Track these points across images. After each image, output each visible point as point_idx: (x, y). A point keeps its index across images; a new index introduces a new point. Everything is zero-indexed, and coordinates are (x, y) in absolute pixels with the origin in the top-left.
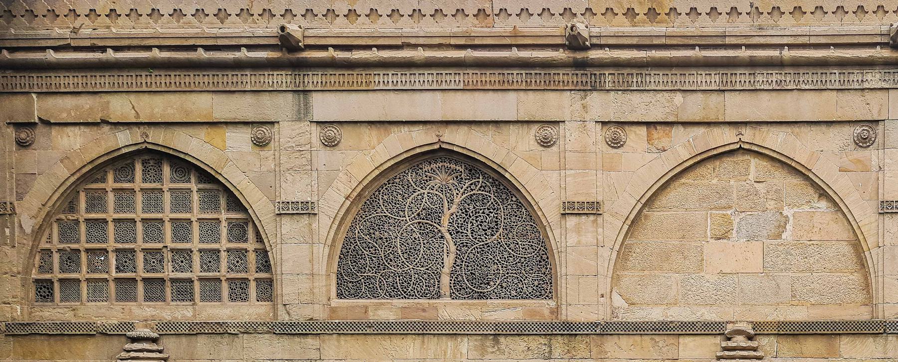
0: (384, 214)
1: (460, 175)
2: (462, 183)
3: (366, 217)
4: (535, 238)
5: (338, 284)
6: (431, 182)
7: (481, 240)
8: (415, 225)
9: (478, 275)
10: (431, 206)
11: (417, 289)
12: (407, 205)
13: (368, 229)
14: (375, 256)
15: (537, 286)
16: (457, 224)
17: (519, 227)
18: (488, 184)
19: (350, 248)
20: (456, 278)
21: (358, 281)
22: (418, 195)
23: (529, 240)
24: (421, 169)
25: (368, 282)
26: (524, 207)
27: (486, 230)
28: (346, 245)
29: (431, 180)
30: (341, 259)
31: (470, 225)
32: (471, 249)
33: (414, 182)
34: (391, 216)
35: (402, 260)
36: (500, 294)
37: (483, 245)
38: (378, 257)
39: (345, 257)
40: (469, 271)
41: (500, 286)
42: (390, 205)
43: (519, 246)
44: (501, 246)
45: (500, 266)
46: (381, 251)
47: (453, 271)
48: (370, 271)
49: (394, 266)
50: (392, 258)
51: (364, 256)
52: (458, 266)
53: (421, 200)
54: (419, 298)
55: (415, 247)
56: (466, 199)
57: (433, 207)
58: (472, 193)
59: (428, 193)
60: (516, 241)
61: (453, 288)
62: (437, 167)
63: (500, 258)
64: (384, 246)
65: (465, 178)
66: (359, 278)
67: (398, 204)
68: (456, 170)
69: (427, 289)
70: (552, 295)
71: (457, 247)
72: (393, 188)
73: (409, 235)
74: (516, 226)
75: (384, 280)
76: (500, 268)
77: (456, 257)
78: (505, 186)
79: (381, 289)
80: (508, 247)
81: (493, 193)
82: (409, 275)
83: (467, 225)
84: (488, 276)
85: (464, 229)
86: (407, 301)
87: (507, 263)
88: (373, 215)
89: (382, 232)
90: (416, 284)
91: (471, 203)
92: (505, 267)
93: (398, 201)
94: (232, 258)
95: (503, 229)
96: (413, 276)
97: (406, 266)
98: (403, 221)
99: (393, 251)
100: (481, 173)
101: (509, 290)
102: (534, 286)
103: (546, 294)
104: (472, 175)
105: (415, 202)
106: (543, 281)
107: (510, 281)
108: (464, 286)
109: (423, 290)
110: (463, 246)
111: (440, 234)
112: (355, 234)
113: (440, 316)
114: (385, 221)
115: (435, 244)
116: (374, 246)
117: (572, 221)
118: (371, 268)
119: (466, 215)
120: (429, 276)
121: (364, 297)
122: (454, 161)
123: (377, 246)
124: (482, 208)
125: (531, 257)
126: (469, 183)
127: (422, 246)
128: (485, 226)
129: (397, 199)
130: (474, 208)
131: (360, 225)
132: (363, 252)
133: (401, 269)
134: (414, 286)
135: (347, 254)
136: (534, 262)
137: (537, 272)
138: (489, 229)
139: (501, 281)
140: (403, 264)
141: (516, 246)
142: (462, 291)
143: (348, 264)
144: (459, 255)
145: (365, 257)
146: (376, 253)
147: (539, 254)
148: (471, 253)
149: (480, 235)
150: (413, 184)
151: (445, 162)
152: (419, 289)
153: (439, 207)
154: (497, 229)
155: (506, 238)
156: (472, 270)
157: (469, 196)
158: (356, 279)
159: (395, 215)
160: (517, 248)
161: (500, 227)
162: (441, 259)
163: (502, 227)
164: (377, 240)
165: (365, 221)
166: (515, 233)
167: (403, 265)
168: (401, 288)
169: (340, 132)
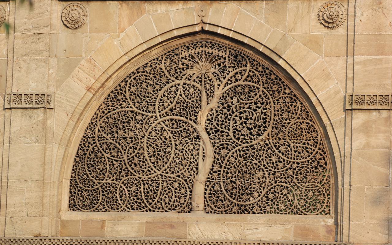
0: (131, 109)
1: (224, 63)
2: (225, 71)
3: (109, 112)
4: (311, 138)
5: (71, 192)
6: (188, 70)
7: (244, 141)
8: (167, 123)
9: (239, 183)
10: (187, 100)
11: (164, 200)
12: (158, 100)
13: (110, 127)
14: (117, 159)
16: (216, 122)
17: (292, 125)
18: (256, 72)
19: (87, 150)
21: (94, 190)
22: (172, 87)
23: (303, 141)
24: (177, 55)
25: (106, 191)
26: (299, 101)
27: (252, 129)
28: (83, 146)
29: (188, 68)
30: (77, 162)
31: (232, 122)
32: (232, 152)
33: (168, 71)
34: (139, 111)
35: (148, 164)
36: (265, 207)
37: (247, 147)
38: (121, 161)
39: (81, 161)
40: (229, 178)
41: (267, 197)
42: (137, 97)
43: (291, 149)
44: (269, 148)
45: (267, 173)
46: (125, 153)
47: (209, 178)
48: (110, 178)
49: (138, 172)
50: (137, 163)
51: (103, 159)
52: (215, 172)
53: (175, 92)
54: (166, 211)
55: (165, 149)
56: (229, 91)
57: (189, 101)
58: (237, 84)
59: (184, 84)
61: (208, 199)
62: (196, 52)
63: (267, 163)
64: (128, 148)
65: (229, 66)
66: (97, 185)
67: (148, 97)
68: (218, 56)
69: (177, 199)
71: (216, 149)
72: (143, 78)
73: (158, 134)
74: (288, 123)
75: (125, 189)
76: (266, 175)
77: (214, 162)
78: (277, 76)
79: (121, 200)
80: (277, 149)
81: (262, 84)
82: (157, 183)
83: (229, 123)
84: (251, 184)
86: (152, 213)
87: (275, 169)
88: (117, 110)
89: (127, 130)
90: (163, 194)
91: (234, 96)
92: (273, 174)
93: (148, 93)
95: (273, 127)
96: (161, 184)
97: (153, 172)
98: (152, 117)
100: (249, 59)
101: (276, 203)
102: (307, 198)
103: (323, 209)
104: (237, 62)
105: (168, 94)
106: (319, 192)
107: (277, 191)
108: (222, 197)
109: (172, 201)
110: (223, 148)
111: (195, 134)
112: (95, 133)
113: (191, 233)
114: (131, 118)
115: (188, 146)
116: (116, 147)
117: (359, 118)
118: (111, 174)
119: (229, 110)
120: (180, 184)
121: (101, 209)
122: (217, 45)
123: (120, 148)
124: (248, 102)
125: (305, 162)
126: (235, 71)
127: (174, 149)
128: (251, 124)
129: (147, 91)
130: (238, 102)
131: (101, 121)
132: (103, 155)
133: (147, 175)
134: (161, 197)
135: (84, 156)
136: (308, 168)
138: (255, 127)
139: (267, 192)
140: (150, 169)
141: (287, 148)
143: (84, 168)
144: (218, 159)
146: (118, 155)
147: (316, 159)
148: (232, 156)
149: (244, 135)
151: (206, 46)
153: (197, 100)
154: (264, 127)
156: (232, 177)
157: (233, 87)
158: (92, 187)
159: (143, 111)
160: (288, 151)
161: (269, 125)
162: (196, 163)
163: (271, 125)
164: (120, 140)
165: (107, 118)
166: (286, 133)
167: (149, 171)
168: (146, 199)
169: (85, 12)
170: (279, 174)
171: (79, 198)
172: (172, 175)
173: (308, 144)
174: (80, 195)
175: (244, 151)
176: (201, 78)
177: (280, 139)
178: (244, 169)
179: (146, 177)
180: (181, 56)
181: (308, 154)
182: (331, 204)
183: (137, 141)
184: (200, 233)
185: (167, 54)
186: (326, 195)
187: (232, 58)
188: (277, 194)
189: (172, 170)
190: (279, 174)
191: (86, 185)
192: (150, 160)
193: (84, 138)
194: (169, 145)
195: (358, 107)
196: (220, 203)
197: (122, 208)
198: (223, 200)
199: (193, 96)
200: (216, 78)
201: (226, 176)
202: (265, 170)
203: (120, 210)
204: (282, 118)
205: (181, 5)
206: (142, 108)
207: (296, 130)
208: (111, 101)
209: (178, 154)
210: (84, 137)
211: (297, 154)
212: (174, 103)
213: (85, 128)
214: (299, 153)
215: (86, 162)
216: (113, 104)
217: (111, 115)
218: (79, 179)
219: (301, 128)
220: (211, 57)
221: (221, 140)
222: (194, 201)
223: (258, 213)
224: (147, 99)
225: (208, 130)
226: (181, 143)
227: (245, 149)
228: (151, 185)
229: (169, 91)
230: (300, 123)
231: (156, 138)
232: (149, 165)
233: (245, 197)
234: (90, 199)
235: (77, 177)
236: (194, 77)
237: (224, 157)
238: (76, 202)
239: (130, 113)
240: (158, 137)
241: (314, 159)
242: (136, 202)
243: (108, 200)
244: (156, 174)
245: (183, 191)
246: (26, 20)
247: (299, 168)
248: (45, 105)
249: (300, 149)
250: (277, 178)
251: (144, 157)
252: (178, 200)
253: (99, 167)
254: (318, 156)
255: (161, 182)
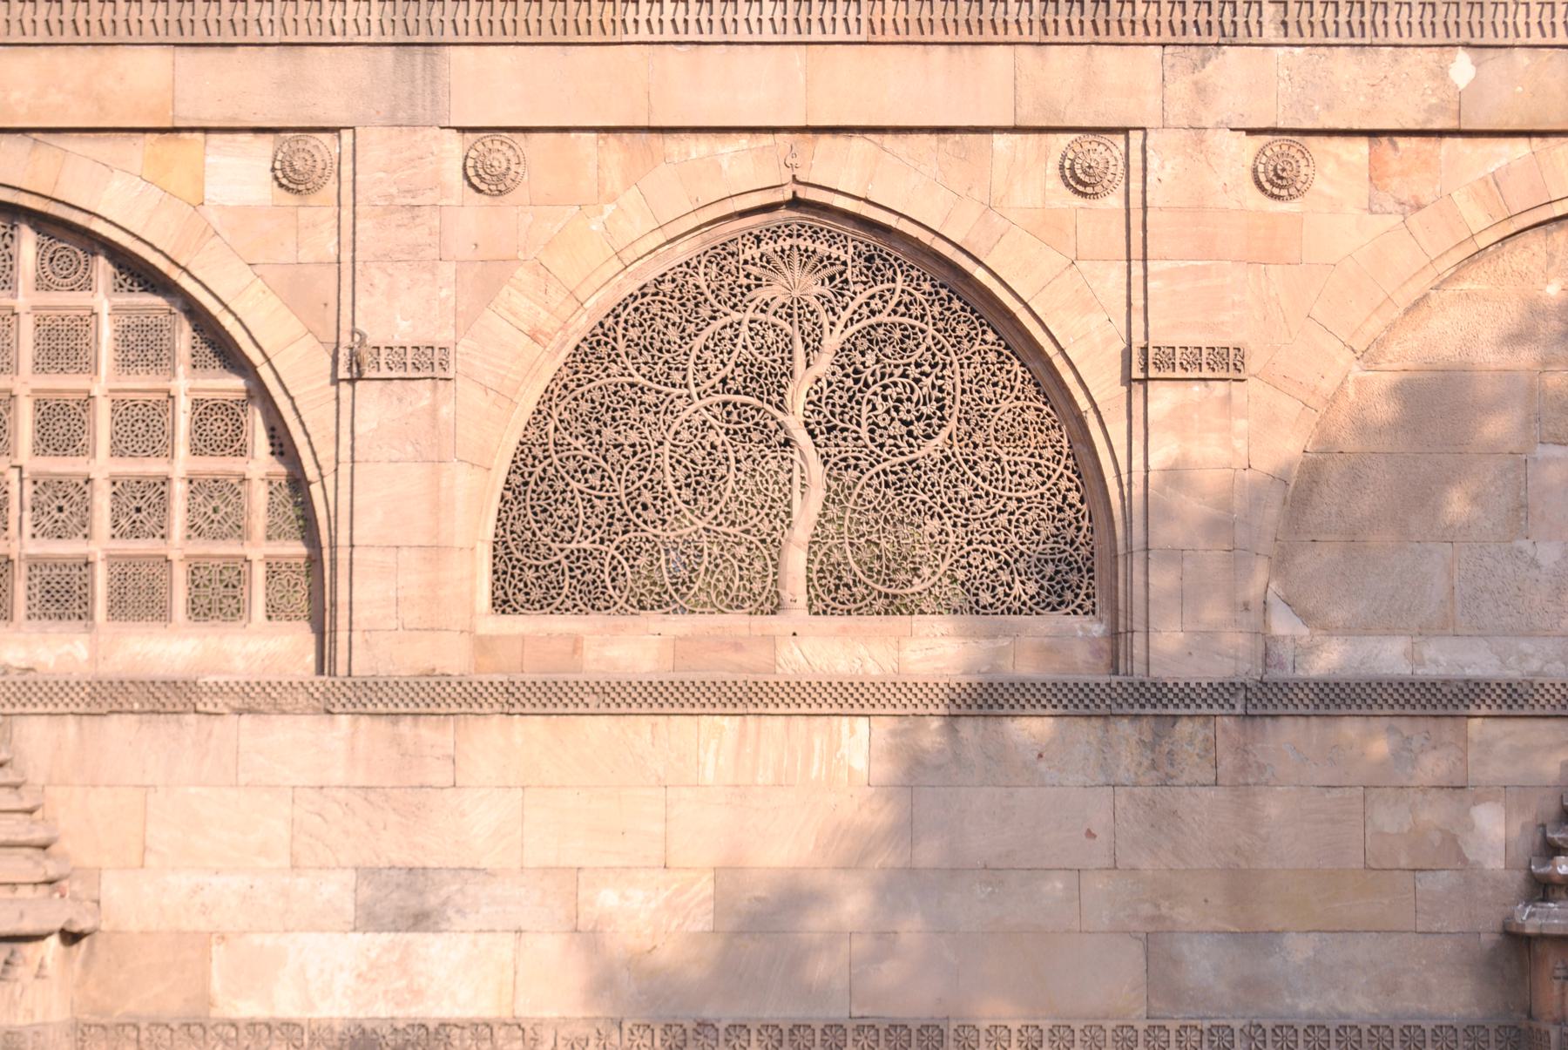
0: (630, 380)
1: (841, 274)
3: (578, 386)
4: (1048, 444)
5: (495, 572)
7: (896, 451)
8: (716, 410)
10: (760, 358)
14: (602, 494)
15: (1051, 579)
18: (918, 295)
19: (531, 474)
20: (825, 554)
21: (551, 566)
22: (724, 327)
23: (1031, 450)
24: (732, 254)
25: (579, 568)
27: (911, 423)
28: (520, 464)
29: (760, 285)
30: (507, 502)
31: (865, 409)
32: (868, 475)
33: (713, 292)
34: (650, 384)
35: (675, 504)
37: (902, 464)
38: (610, 498)
40: (863, 535)
41: (949, 577)
42: (644, 352)
43: (1003, 469)
44: (952, 467)
45: (949, 523)
46: (619, 480)
48: (586, 538)
50: (649, 501)
52: (831, 521)
53: (731, 339)
55: (714, 471)
57: (766, 359)
58: (873, 321)
59: (751, 322)
60: (995, 454)
62: (778, 249)
63: (950, 500)
67: (668, 351)
68: (829, 258)
70: (1094, 605)
71: (831, 469)
72: (655, 308)
73: (695, 436)
74: (995, 410)
75: (624, 562)
76: (949, 528)
77: (827, 499)
79: (614, 588)
80: (971, 468)
81: (931, 321)
82: (696, 547)
83: (859, 410)
85: (850, 421)
86: (688, 617)
88: (598, 383)
89: (622, 428)
90: (713, 572)
91: (869, 348)
92: (963, 526)
93: (669, 342)
94: (200, 499)
95: (959, 420)
96: (706, 551)
98: (680, 397)
99: (651, 480)
100: (900, 266)
101: (973, 590)
103: (1078, 601)
105: (716, 345)
106: (1069, 564)
107: (974, 564)
108: (848, 579)
111: (782, 434)
113: (781, 661)
116: (598, 467)
118: (589, 527)
119: (856, 381)
120: (749, 549)
121: (567, 610)
122: (825, 232)
123: (608, 468)
126: (870, 292)
127: (733, 469)
130: (878, 361)
131: (561, 408)
132: (567, 485)
133: (674, 530)
135: (522, 488)
136: (1043, 511)
137: (1052, 539)
138: (918, 419)
139: (952, 565)
142: (843, 591)
143: (525, 516)
145: (573, 498)
146: (602, 486)
147: (1059, 490)
148: (869, 485)
149: (894, 438)
150: (711, 298)
151: (799, 236)
152: (722, 587)
153: (782, 358)
154: (942, 418)
155: (967, 445)
156: (870, 533)
158: (545, 558)
159: (659, 383)
161: (950, 415)
162: (785, 502)
164: (607, 450)
165: (575, 399)
168: (673, 584)
170: (977, 525)
171: (515, 586)
172: (731, 530)
173: (1041, 456)
174: (517, 578)
175: (895, 473)
176: (791, 308)
177: (976, 446)
178: (898, 514)
179: (672, 535)
180: (742, 258)
181: (1040, 479)
182: (1097, 592)
183: (647, 453)
184: (803, 661)
185: (711, 252)
186: (1084, 569)
187: (861, 262)
188: (974, 570)
189: (731, 517)
190: (977, 525)
191: (530, 555)
192: (679, 495)
193: (521, 447)
194: (723, 461)
195: (1161, 375)
196: (843, 591)
197: (618, 606)
198: (851, 583)
199: (774, 348)
200: (826, 306)
201: (858, 531)
202: (945, 516)
203: (613, 610)
204: (981, 399)
205: (744, 141)
206: (656, 376)
207: (1012, 426)
208: (583, 361)
209: (744, 482)
210: (522, 443)
211: (1016, 479)
212: (731, 365)
213: (524, 424)
214: (1021, 477)
215: (528, 502)
216: (588, 367)
217: (583, 395)
218: (514, 540)
219: (1024, 421)
220: (814, 260)
221: (843, 449)
222: (784, 588)
223: (934, 613)
224: (667, 356)
225: (811, 427)
226: (749, 456)
227: (898, 468)
228: (683, 553)
229: (717, 337)
230: (1022, 409)
231: (691, 445)
232: (677, 508)
233: (902, 577)
234: (540, 586)
235: (509, 537)
236: (775, 305)
237: (849, 488)
238: (510, 593)
239: (627, 387)
240: (695, 442)
241: (1054, 490)
242: (651, 592)
243: (584, 588)
244: (694, 528)
245: (758, 565)
246: (382, 175)
247: (1022, 510)
248: (439, 373)
249: (1023, 469)
250: (972, 533)
251: (664, 488)
252: (748, 585)
253: (559, 513)
254: (1064, 484)
255: (706, 545)
